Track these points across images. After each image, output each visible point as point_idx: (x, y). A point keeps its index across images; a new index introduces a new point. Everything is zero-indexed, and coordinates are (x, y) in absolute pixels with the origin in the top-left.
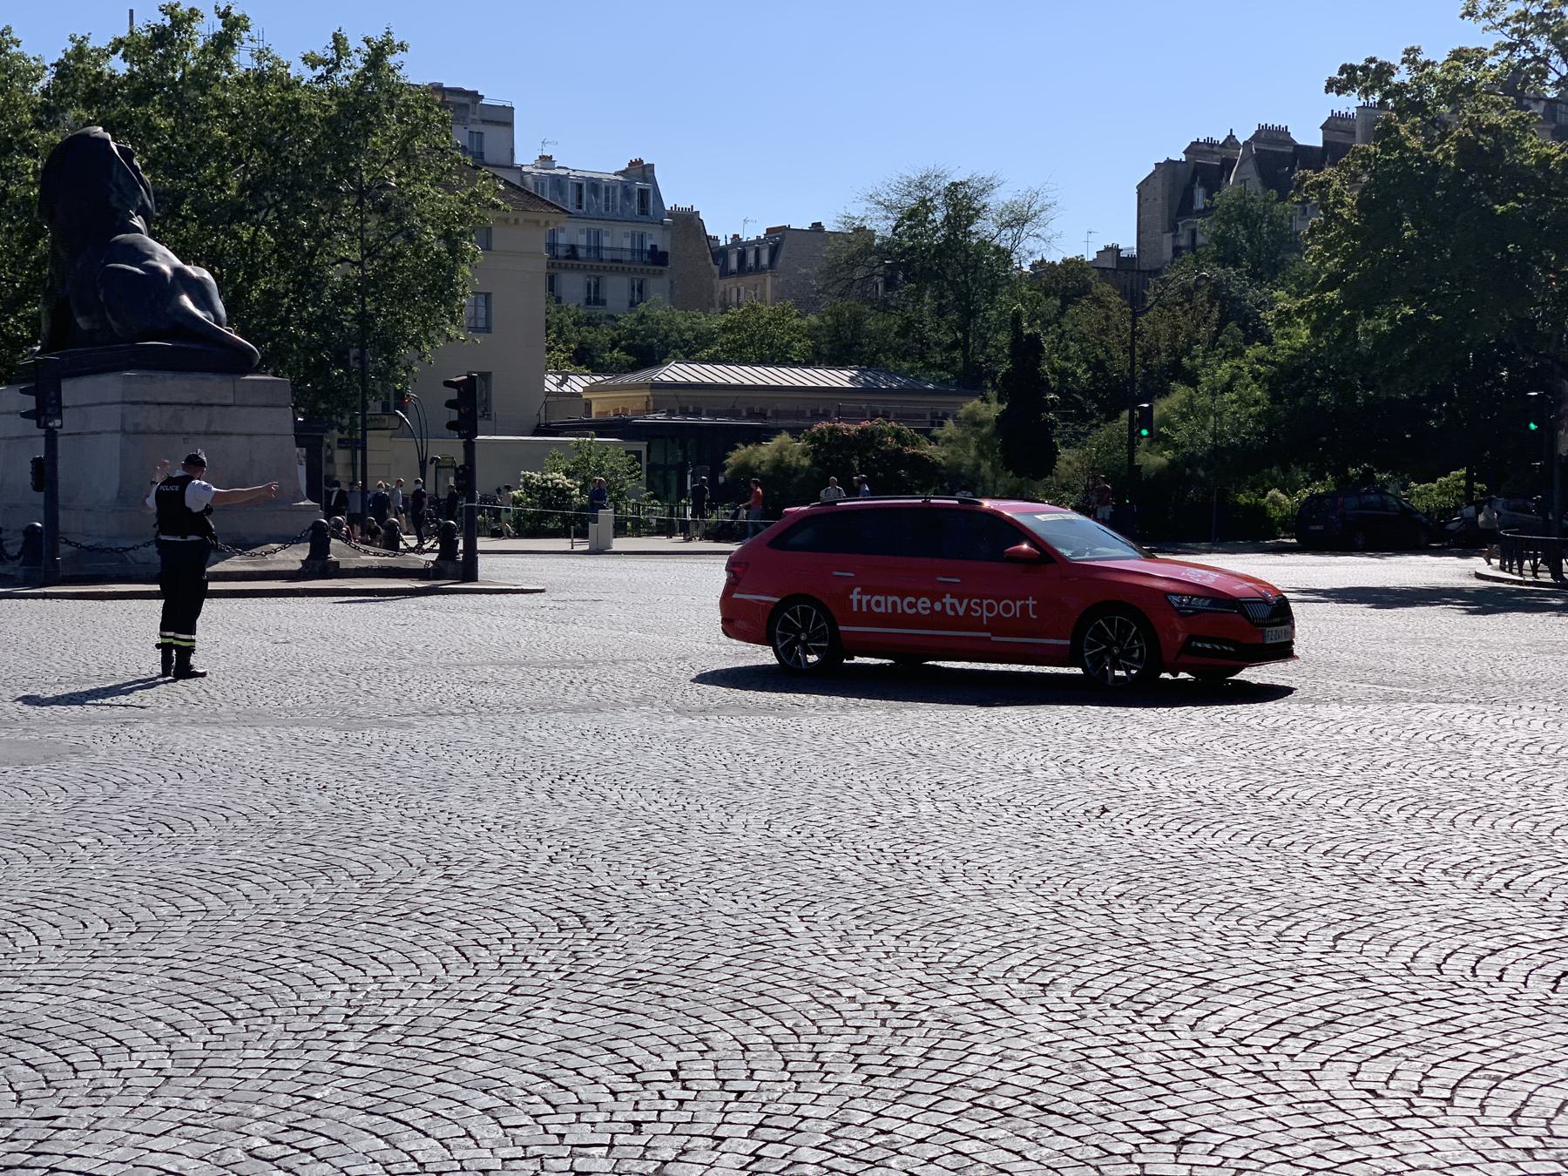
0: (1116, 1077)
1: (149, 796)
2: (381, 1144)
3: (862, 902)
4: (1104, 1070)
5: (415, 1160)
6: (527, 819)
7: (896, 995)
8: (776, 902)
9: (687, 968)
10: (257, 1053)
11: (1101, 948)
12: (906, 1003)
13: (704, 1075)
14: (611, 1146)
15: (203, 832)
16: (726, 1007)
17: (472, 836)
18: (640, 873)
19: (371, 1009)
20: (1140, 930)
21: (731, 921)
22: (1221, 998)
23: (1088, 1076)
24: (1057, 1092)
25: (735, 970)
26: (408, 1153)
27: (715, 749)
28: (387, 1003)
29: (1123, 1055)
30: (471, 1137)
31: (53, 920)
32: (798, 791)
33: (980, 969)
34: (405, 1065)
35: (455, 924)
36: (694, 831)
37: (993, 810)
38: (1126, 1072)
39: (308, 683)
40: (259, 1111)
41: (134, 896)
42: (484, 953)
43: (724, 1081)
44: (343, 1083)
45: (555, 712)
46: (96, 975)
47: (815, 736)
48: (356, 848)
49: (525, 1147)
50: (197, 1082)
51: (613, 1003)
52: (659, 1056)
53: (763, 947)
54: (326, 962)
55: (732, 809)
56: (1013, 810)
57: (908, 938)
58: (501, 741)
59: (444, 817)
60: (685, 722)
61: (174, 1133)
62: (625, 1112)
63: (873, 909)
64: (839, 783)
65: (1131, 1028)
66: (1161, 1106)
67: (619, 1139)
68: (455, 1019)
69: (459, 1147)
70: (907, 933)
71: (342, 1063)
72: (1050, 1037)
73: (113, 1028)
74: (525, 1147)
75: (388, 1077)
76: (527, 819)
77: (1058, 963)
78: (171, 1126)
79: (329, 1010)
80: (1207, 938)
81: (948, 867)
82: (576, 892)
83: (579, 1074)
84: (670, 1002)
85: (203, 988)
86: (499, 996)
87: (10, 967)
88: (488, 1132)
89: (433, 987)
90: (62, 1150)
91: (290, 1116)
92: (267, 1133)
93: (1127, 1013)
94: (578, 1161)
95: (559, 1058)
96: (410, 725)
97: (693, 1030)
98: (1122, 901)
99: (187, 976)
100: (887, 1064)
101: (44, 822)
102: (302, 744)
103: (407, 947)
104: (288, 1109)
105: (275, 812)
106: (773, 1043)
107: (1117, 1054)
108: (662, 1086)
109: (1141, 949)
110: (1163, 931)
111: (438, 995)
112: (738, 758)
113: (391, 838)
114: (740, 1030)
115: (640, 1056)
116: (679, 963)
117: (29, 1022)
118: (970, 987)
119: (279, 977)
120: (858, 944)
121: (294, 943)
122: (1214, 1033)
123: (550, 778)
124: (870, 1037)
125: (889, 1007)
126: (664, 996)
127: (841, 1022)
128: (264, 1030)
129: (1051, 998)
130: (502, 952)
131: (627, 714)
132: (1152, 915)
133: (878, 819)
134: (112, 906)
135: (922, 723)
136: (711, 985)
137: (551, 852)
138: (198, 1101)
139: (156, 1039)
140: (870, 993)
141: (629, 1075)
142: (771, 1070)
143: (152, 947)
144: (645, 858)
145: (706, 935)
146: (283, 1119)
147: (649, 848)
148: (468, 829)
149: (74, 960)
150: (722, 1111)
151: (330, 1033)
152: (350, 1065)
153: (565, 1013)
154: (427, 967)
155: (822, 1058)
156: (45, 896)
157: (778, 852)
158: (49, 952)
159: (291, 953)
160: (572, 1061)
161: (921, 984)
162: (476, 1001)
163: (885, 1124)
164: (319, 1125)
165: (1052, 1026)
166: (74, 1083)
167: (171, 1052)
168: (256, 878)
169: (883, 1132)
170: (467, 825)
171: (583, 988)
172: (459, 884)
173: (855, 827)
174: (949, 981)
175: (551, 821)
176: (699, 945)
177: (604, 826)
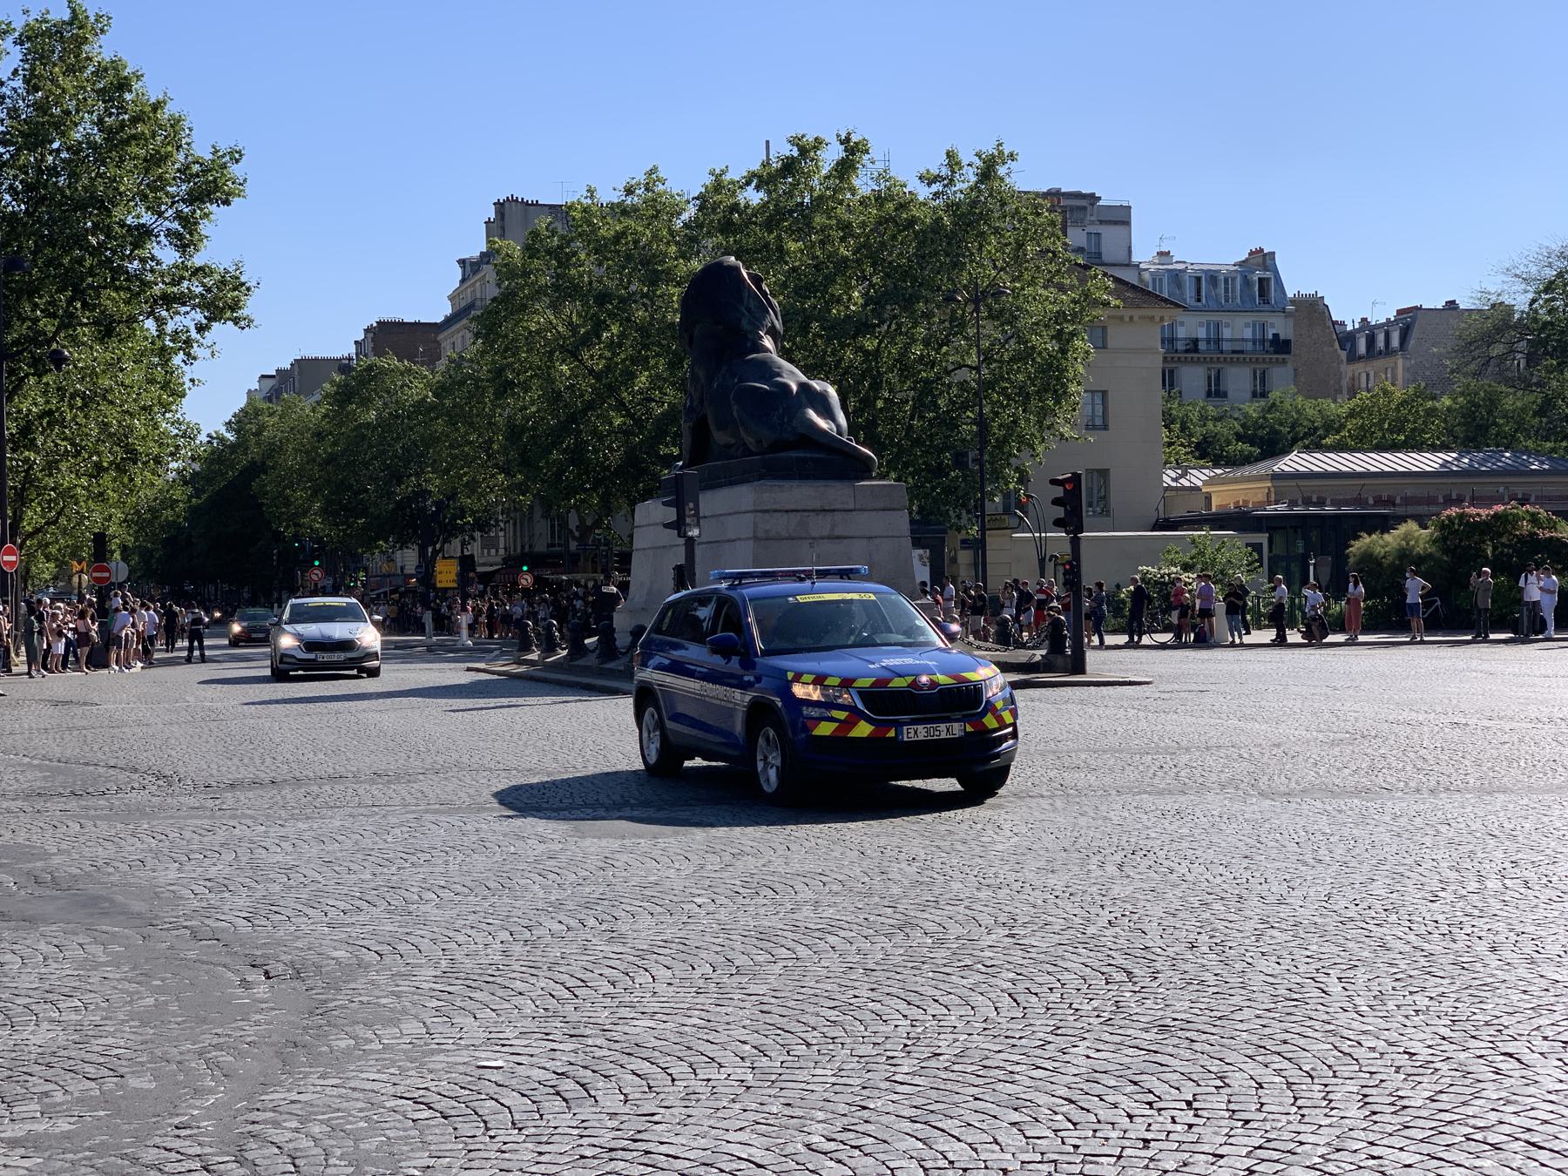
2: (920, 1145)
3: (1404, 967)
5: (946, 1158)
6: (1094, 889)
7: (1416, 1047)
8: (1318, 965)
9: (1220, 1018)
10: (826, 1072)
14: (1119, 1157)
16: (1249, 1052)
17: (1040, 902)
18: (1192, 936)
19: (927, 1041)
24: (1551, 1132)
25: (1264, 1022)
26: (941, 1153)
27: (1291, 829)
28: (941, 1036)
30: (997, 1143)
31: (667, 963)
32: (1366, 868)
33: (1506, 1027)
34: (949, 1086)
40: (820, 1115)
41: (738, 946)
42: (1034, 999)
43: (1234, 1111)
44: (895, 1097)
45: (1139, 793)
46: (698, 1007)
47: (1395, 817)
48: (933, 911)
49: (1042, 1154)
51: (1144, 1045)
54: (894, 1002)
55: (1294, 884)
57: (1442, 999)
58: (1083, 821)
59: (1016, 886)
61: (748, 1130)
62: (1138, 1130)
63: (1413, 973)
67: (1127, 1152)
69: (987, 1150)
70: (1442, 995)
72: (1559, 1086)
73: (709, 1049)
74: (1042, 1154)
75: (934, 1094)
76: (1094, 889)
78: (747, 1124)
79: (890, 1040)
81: (1501, 938)
82: (1128, 951)
84: (1196, 1046)
85: (786, 1019)
86: (1041, 1035)
87: (628, 999)
88: (1012, 1139)
89: (984, 1025)
90: (657, 1139)
91: (845, 1121)
92: (825, 1133)
94: (1088, 1166)
95: (1085, 1086)
100: (1392, 1104)
101: (668, 883)
103: (967, 992)
105: (866, 879)
108: (1175, 1113)
111: (987, 1032)
112: (1312, 837)
113: (966, 903)
114: (1261, 1070)
115: (1160, 1088)
116: (1212, 1014)
120: (1390, 1003)
121: (868, 986)
123: (1122, 854)
124: (1382, 1081)
125: (1407, 1056)
127: (1357, 1068)
130: (1050, 999)
131: (1210, 797)
133: (1442, 894)
135: (1511, 806)
139: (742, 1058)
140: (1391, 1044)
141: (1147, 1103)
145: (1243, 992)
146: (840, 1123)
147: (1207, 915)
151: (889, 1058)
155: (1331, 1096)
157: (1331, 922)
158: (661, 988)
160: (1098, 1089)
161: (1444, 1039)
163: (1376, 1151)
164: (870, 1128)
166: (671, 1089)
168: (842, 933)
169: (1374, 1158)
170: (1038, 893)
171: (1119, 1031)
174: (1473, 1037)
175: (1116, 890)
176: (1234, 1000)
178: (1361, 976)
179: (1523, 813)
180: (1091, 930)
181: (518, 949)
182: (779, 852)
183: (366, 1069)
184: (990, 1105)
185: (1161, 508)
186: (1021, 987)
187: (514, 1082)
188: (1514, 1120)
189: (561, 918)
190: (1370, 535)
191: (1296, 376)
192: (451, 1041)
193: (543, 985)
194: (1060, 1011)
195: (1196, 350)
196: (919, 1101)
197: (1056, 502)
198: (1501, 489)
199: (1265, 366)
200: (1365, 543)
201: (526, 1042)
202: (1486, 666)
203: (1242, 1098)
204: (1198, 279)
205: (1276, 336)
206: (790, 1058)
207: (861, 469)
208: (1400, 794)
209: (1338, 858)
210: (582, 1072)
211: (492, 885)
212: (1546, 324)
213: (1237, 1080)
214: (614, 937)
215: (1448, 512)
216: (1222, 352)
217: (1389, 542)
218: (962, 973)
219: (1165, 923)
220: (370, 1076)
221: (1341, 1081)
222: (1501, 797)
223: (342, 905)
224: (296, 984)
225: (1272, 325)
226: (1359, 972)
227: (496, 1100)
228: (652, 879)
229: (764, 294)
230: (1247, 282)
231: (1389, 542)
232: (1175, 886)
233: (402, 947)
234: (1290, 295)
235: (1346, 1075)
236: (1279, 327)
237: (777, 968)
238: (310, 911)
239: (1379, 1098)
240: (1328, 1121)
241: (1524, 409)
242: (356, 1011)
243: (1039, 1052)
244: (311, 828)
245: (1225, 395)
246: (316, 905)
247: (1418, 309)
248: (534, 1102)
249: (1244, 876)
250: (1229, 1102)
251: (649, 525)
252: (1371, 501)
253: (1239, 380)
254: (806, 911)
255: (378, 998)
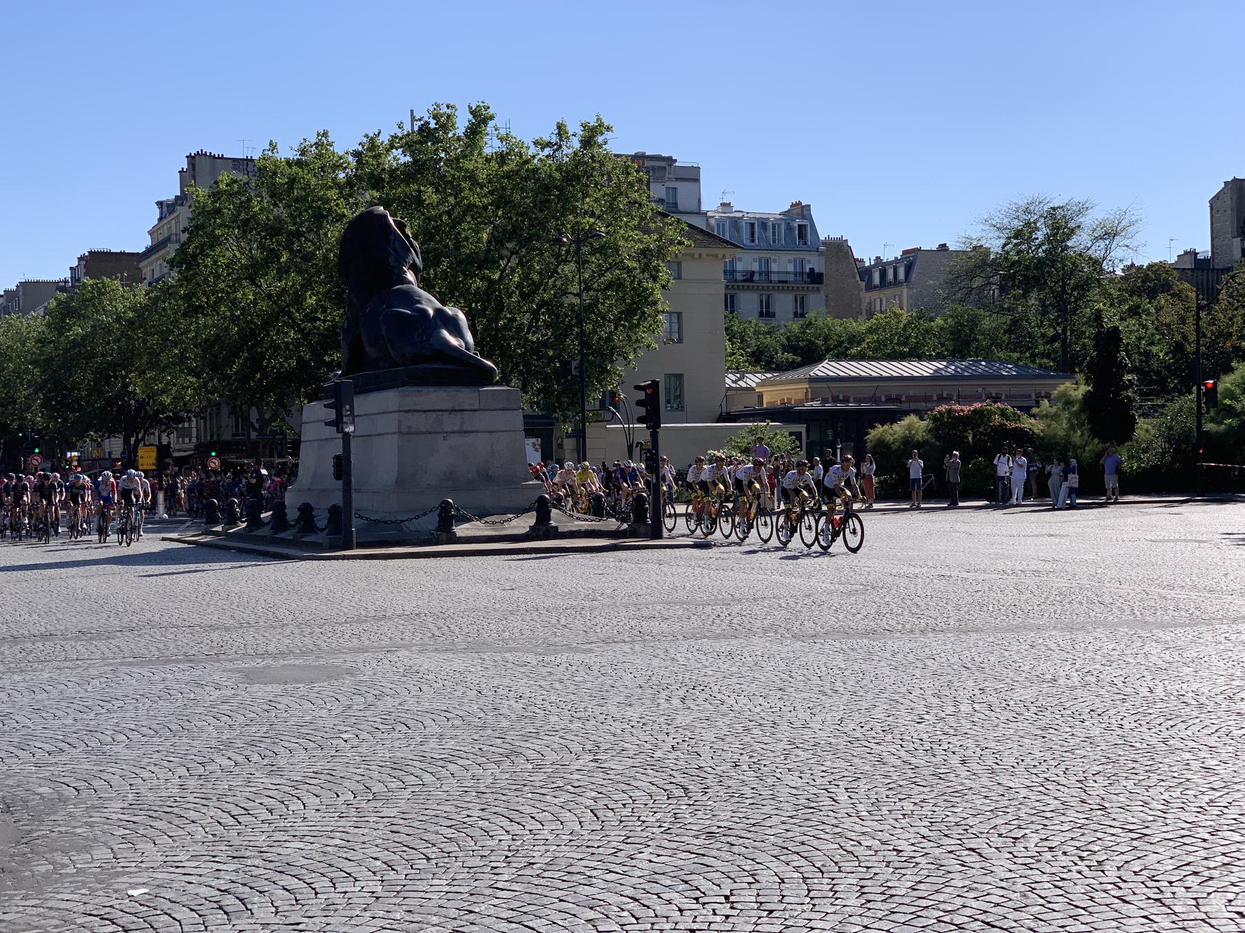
0: (1049, 902)
1: (396, 704)
4: (1042, 898)
6: (662, 719)
7: (903, 845)
8: (831, 778)
9: (754, 825)
10: (441, 883)
11: (1068, 812)
12: (908, 850)
13: (748, 899)
15: (430, 730)
16: (775, 853)
17: (619, 731)
20: (1103, 799)
21: (794, 791)
22: (1149, 847)
23: (1028, 902)
27: (815, 665)
28: (536, 848)
29: (1060, 888)
31: (316, 792)
32: (870, 696)
33: (971, 827)
34: (540, 891)
35: (594, 794)
36: (784, 726)
37: (1017, 709)
38: (1060, 899)
39: (523, 620)
40: (435, 920)
41: (376, 775)
42: (610, 814)
43: (761, 903)
44: (496, 902)
45: (701, 638)
46: (340, 829)
50: (397, 901)
51: (695, 849)
52: (719, 886)
53: (812, 810)
55: (815, 711)
56: (1034, 709)
57: (923, 804)
58: (655, 662)
60: (798, 644)
63: (902, 783)
64: (903, 689)
65: (1072, 868)
66: (1076, 922)
68: (581, 859)
70: (924, 801)
71: (497, 888)
72: (1009, 875)
75: (527, 898)
76: (662, 719)
77: (1032, 822)
79: (495, 853)
80: (1154, 805)
81: (970, 753)
82: (686, 771)
83: (659, 897)
84: (735, 849)
85: (411, 838)
87: (282, 824)
93: (1072, 858)
95: (647, 886)
96: (591, 651)
97: (747, 868)
98: (1095, 778)
99: (402, 829)
100: (883, 893)
102: (510, 665)
104: (455, 919)
105: (482, 715)
106: (804, 878)
107: (1056, 886)
109: (1099, 812)
110: (1122, 799)
111: (572, 843)
112: (831, 672)
114: (784, 868)
115: (706, 886)
116: (748, 822)
117: (290, 861)
118: (960, 839)
119: (465, 830)
120: (884, 808)
122: (1134, 872)
124: (875, 874)
125: (895, 853)
126: (732, 845)
127: (857, 864)
128: (448, 866)
129: (1020, 846)
130: (623, 814)
131: (755, 640)
132: (1117, 788)
133: (927, 717)
134: (358, 782)
136: (767, 837)
137: (674, 742)
138: (395, 914)
139: (374, 873)
140: (883, 843)
142: (798, 896)
143: (381, 810)
144: (741, 746)
145: (772, 802)
147: (748, 739)
148: (617, 727)
149: (327, 819)
150: (754, 923)
151: (493, 868)
152: (502, 890)
153: (659, 855)
154: (569, 824)
155: (836, 888)
156: (314, 775)
158: (310, 814)
159: (477, 813)
160: (657, 888)
161: (924, 837)
162: (598, 847)
165: (1013, 867)
166: (314, 901)
167: (382, 881)
168: (460, 762)
170: (618, 723)
171: (676, 839)
172: (602, 766)
173: (906, 723)
174: (945, 835)
175: (680, 720)
176: (767, 809)
177: (717, 723)
178: (863, 786)
179: (990, 648)
180: (658, 754)
181: (192, 783)
182: (413, 693)
183: (61, 890)
184: (571, 905)
185: (724, 404)
186: (601, 804)
187: (184, 898)
188: (974, 904)
189: (230, 754)
190: (883, 426)
191: (827, 301)
192: (133, 864)
193: (212, 814)
194: (630, 823)
195: (751, 280)
196: (515, 904)
197: (639, 403)
198: (980, 390)
199: (803, 293)
200: (878, 432)
201: (196, 864)
202: (967, 528)
203: (768, 892)
204: (752, 225)
205: (812, 270)
206: (413, 871)
207: (485, 377)
208: (899, 634)
209: (850, 688)
210: (241, 889)
211: (173, 728)
212: (1014, 264)
213: (765, 877)
214: (274, 770)
215: (940, 408)
216: (771, 282)
217: (898, 429)
218: (555, 794)
219: (716, 746)
220: (64, 898)
221: (844, 875)
222: (974, 636)
223: (47, 747)
224: (6, 817)
225: (809, 262)
226: (861, 783)
227: (169, 915)
228: (308, 718)
229: (407, 237)
230: (789, 228)
231: (898, 429)
232: (725, 715)
233: (97, 783)
234: (822, 238)
235: (848, 870)
236: (814, 263)
237: (406, 794)
238: (20, 753)
239: (873, 888)
240: (833, 909)
241: (997, 329)
242: (55, 840)
243: (612, 858)
244: (24, 681)
245: (773, 315)
246: (26, 747)
247: (919, 250)
248: (200, 916)
249: (778, 705)
250: (758, 895)
251: (314, 422)
252: (883, 399)
253: (783, 304)
254: (433, 744)
255: (74, 827)
